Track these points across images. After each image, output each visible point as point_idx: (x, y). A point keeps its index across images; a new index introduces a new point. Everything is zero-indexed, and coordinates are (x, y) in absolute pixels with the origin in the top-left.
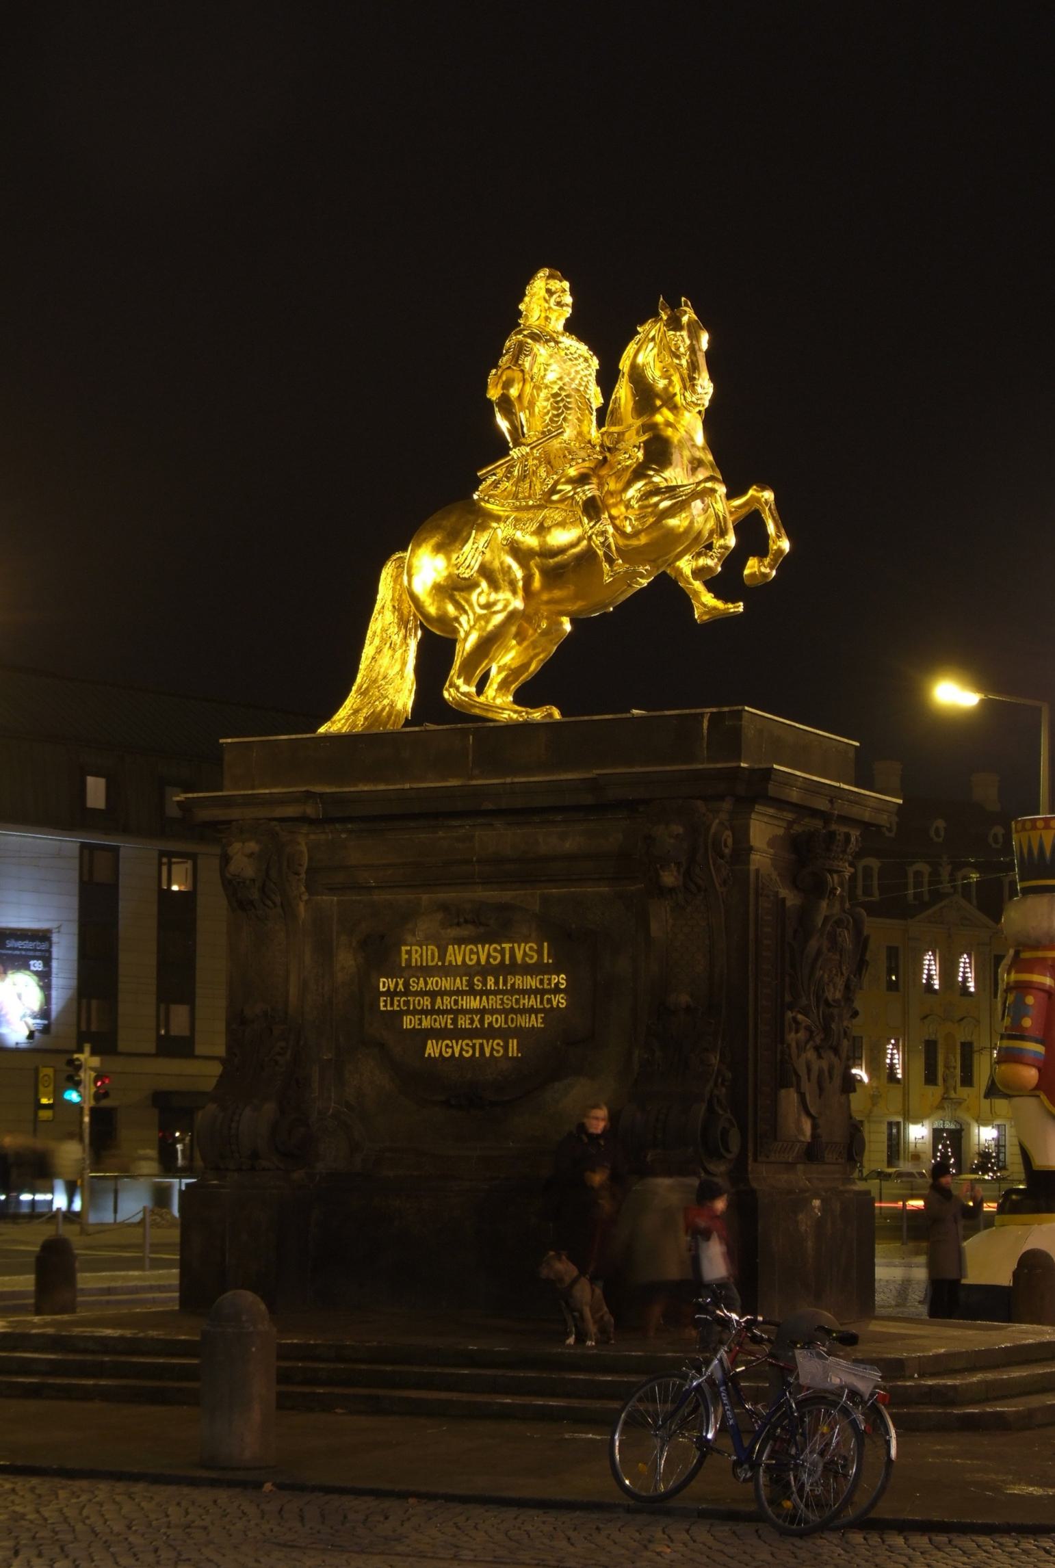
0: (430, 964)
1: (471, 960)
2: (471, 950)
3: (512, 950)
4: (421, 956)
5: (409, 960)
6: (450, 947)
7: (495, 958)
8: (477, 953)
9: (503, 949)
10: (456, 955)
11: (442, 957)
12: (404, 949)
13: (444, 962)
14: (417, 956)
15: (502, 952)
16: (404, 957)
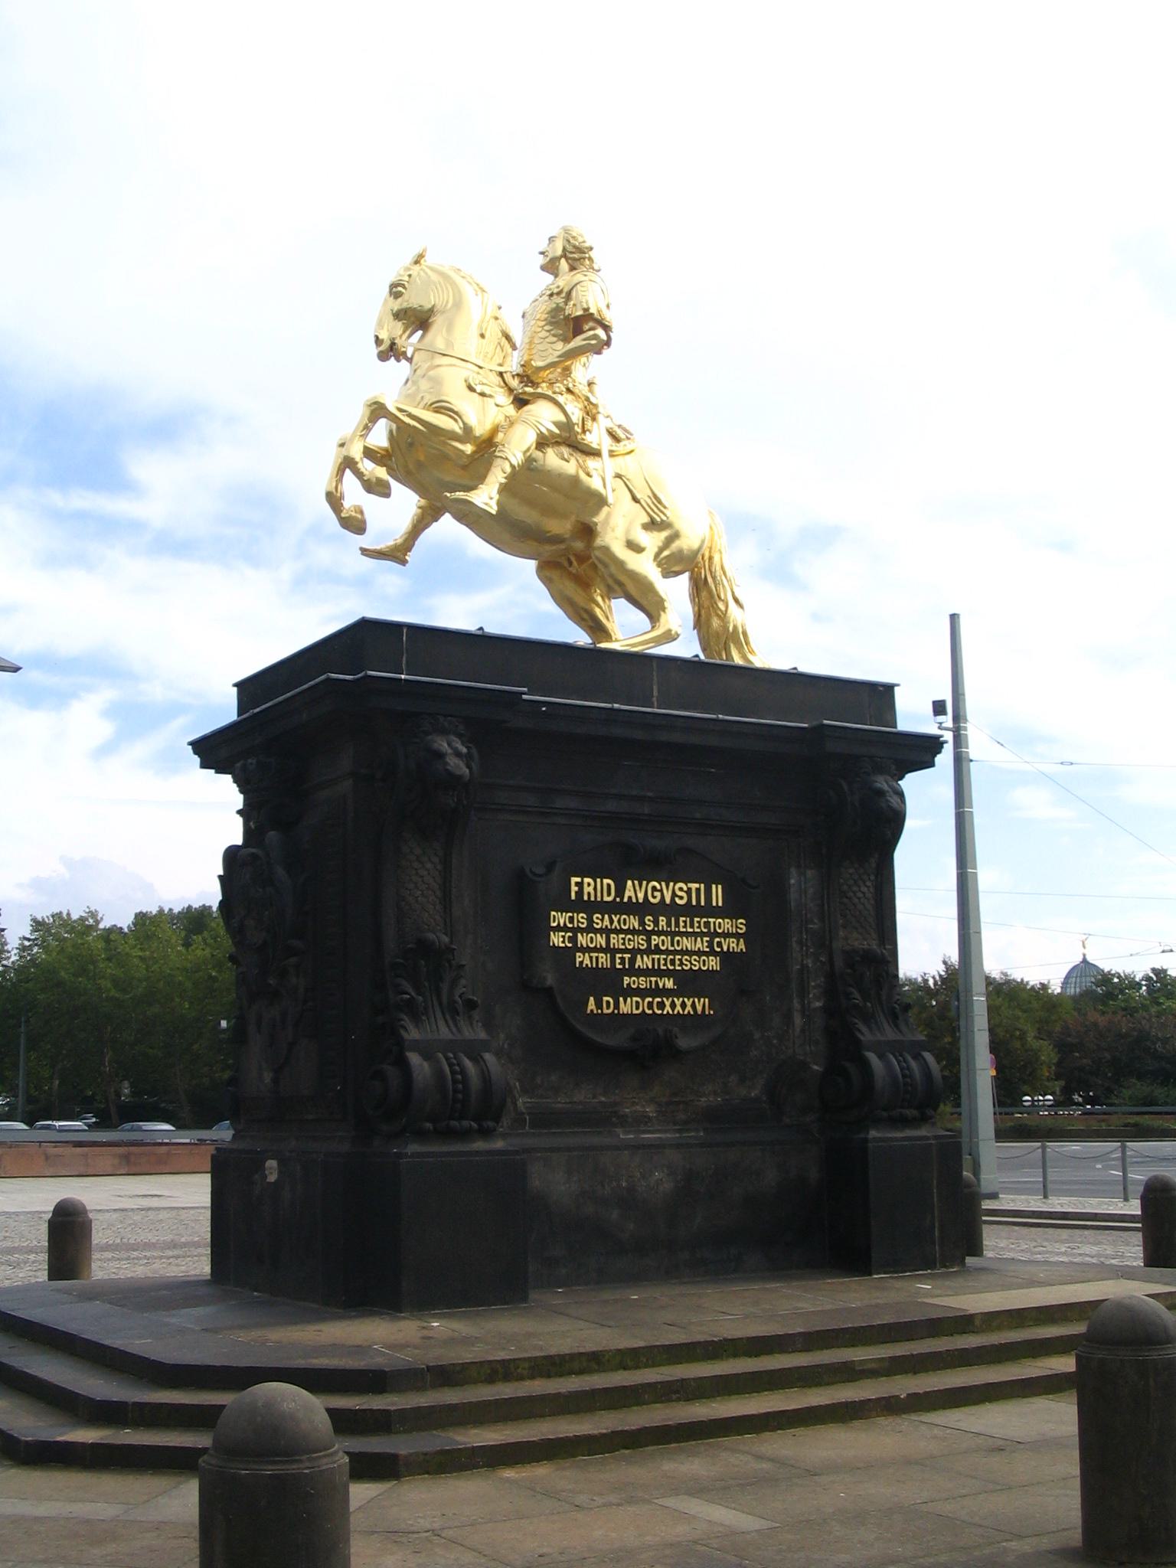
0: (607, 899)
1: (654, 897)
2: (654, 889)
3: (698, 890)
4: (595, 889)
5: (580, 893)
6: (629, 883)
7: (681, 898)
8: (661, 891)
9: (690, 889)
10: (633, 891)
11: (620, 891)
12: (575, 880)
13: (622, 898)
14: (591, 889)
15: (689, 892)
16: (574, 889)
